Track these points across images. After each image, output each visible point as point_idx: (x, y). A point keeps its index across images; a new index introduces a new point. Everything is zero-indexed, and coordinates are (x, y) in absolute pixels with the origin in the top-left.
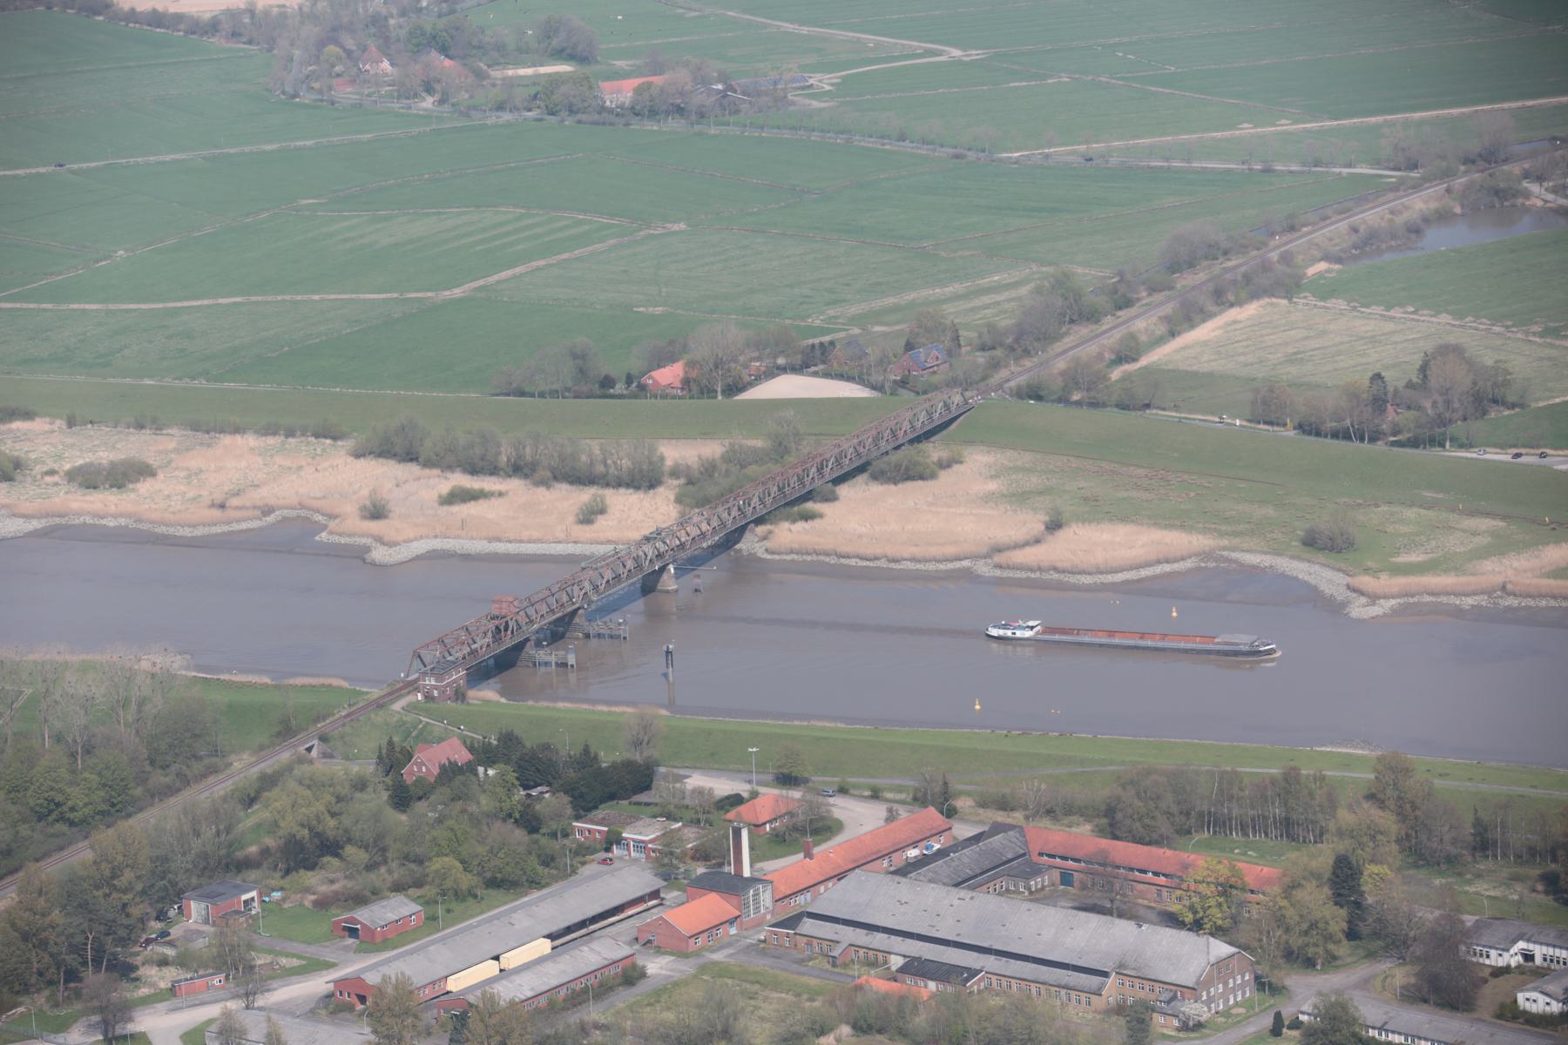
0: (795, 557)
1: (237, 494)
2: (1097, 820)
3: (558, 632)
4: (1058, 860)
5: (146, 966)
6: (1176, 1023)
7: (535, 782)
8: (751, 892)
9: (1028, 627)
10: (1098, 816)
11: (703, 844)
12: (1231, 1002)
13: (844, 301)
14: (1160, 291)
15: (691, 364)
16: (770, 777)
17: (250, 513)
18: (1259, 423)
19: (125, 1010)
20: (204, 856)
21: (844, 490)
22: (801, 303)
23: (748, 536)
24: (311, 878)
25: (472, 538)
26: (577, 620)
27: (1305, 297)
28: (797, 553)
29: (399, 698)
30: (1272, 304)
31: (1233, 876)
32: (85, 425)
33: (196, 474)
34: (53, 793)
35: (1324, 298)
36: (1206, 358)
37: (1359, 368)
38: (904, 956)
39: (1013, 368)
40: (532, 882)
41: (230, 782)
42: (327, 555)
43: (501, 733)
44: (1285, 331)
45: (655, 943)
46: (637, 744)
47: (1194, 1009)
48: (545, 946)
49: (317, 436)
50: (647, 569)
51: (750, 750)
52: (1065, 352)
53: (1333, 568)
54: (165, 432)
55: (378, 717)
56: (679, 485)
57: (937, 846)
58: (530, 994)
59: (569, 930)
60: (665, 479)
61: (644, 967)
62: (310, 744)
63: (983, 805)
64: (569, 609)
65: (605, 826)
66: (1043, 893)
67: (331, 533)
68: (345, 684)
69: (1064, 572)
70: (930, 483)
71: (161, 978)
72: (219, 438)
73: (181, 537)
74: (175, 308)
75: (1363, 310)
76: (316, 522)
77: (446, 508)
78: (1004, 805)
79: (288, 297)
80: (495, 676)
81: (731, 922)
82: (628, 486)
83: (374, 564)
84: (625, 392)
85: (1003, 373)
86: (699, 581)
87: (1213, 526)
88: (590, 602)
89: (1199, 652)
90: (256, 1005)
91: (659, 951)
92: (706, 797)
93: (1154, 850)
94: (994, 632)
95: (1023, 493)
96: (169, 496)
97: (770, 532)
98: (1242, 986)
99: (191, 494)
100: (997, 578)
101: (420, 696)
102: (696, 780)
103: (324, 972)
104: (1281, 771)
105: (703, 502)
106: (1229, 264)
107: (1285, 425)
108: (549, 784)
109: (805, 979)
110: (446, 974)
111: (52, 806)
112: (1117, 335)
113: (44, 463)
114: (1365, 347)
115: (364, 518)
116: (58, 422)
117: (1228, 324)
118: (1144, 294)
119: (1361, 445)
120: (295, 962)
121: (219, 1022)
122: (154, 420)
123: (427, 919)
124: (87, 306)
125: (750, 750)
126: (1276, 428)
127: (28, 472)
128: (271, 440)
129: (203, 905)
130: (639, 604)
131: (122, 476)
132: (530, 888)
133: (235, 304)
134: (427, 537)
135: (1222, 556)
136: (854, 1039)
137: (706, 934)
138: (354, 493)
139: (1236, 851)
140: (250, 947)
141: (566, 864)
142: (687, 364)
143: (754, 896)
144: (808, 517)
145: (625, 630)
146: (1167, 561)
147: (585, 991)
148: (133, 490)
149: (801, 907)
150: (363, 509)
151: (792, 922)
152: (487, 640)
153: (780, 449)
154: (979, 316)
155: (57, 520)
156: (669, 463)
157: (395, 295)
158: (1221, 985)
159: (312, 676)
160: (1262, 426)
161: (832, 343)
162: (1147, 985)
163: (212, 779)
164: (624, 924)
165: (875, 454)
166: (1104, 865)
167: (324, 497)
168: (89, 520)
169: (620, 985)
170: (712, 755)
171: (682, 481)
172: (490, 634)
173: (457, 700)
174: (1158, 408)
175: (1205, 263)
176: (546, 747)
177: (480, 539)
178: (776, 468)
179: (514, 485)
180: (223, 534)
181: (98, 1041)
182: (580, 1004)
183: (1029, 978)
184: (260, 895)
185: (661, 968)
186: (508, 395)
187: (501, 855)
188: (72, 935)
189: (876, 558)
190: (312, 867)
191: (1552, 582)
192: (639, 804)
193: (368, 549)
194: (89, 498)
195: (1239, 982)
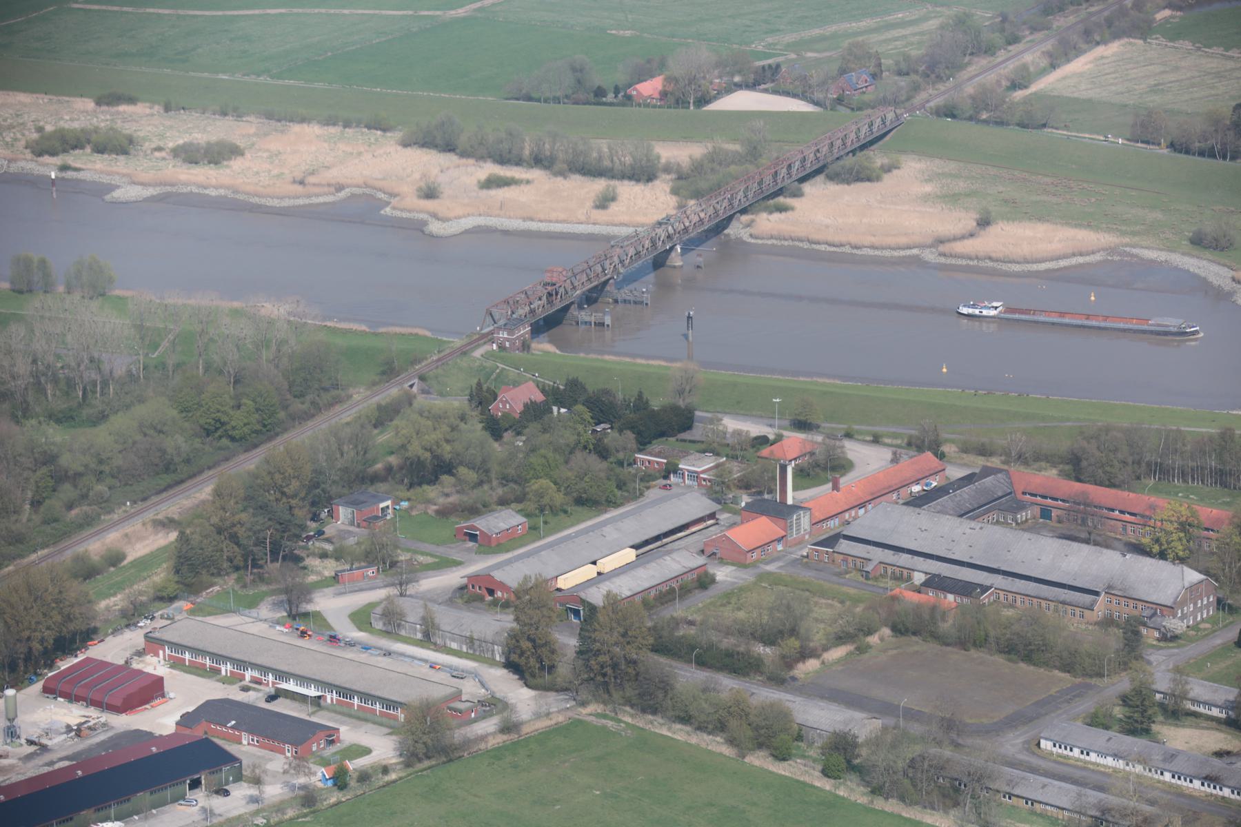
0: (774, 242)
1: (312, 173)
2: (1061, 466)
3: (591, 298)
4: (1039, 498)
5: (310, 558)
6: (1157, 634)
7: (599, 420)
8: (795, 517)
9: (993, 307)
10: (1060, 463)
11: (744, 475)
12: (1199, 619)
13: (778, 30)
14: (1040, 30)
15: (668, 80)
16: (787, 423)
17: (326, 189)
18: (1138, 142)
19: (306, 592)
20: (345, 470)
21: (807, 188)
22: (744, 32)
24: (431, 491)
25: (510, 217)
26: (608, 288)
27: (1156, 39)
28: (776, 239)
29: (479, 346)
30: (1130, 44)
31: (1192, 516)
32: (179, 110)
33: (276, 155)
34: (219, 414)
35: (1171, 40)
36: (1083, 87)
37: (1211, 98)
38: (926, 573)
39: (931, 91)
40: (610, 502)
41: (354, 411)
42: (392, 226)
43: (568, 379)
44: (1144, 66)
45: (718, 556)
46: (681, 393)
47: (1175, 625)
48: (629, 555)
49: (369, 127)
50: (660, 248)
51: (774, 400)
52: (971, 79)
53: (1219, 264)
54: (244, 119)
55: (464, 363)
56: (671, 180)
57: (934, 484)
58: (629, 593)
59: (647, 543)
60: (659, 174)
61: (714, 574)
62: (412, 382)
63: (965, 450)
64: (603, 279)
65: (665, 458)
66: (1027, 524)
67: (394, 208)
68: (428, 334)
69: (997, 260)
70: (875, 184)
71: (328, 568)
72: (290, 126)
73: (271, 207)
74: (233, 16)
75: (1207, 50)
76: (379, 199)
77: (485, 193)
78: (983, 451)
79: (323, 11)
80: (543, 332)
81: (779, 540)
82: (631, 178)
83: (431, 236)
84: (615, 100)
85: (923, 96)
86: (701, 259)
87: (1115, 227)
88: (619, 273)
89: (1136, 331)
90: (408, 593)
91: (722, 562)
92: (743, 438)
93: (1113, 491)
94: (965, 310)
95: (953, 195)
96: (257, 173)
97: (753, 221)
98: (1207, 607)
99: (275, 172)
100: (939, 263)
101: (495, 347)
102: (731, 424)
103: (454, 569)
104: (1219, 431)
105: (697, 195)
106: (1093, 9)
107: (1159, 144)
108: (611, 422)
109: (845, 589)
110: (556, 574)
111: (218, 425)
112: (1011, 66)
113: (150, 140)
114: (1214, 81)
115: (420, 197)
116: (157, 107)
117: (1096, 59)
118: (1027, 33)
119: (1224, 162)
120: (430, 560)
121: (383, 605)
122: (235, 109)
123: (530, 528)
124: (160, 11)
125: (774, 400)
126: (1152, 147)
127: (139, 148)
128: (332, 130)
129: (350, 510)
130: (651, 277)
131: (218, 154)
132: (609, 506)
133: (281, 14)
134: (473, 215)
135: (1125, 251)
136: (894, 640)
137: (760, 550)
138: (408, 176)
139: (1180, 495)
140: (396, 547)
141: (635, 488)
142: (665, 79)
143: (797, 520)
144: (782, 209)
145: (647, 298)
146: (1081, 255)
147: (672, 590)
148: (227, 167)
149: (832, 530)
150: (419, 189)
151: (831, 541)
152: (542, 302)
153: (753, 153)
154: (890, 47)
155: (169, 189)
156: (663, 161)
157: (411, 13)
158: (1192, 605)
159: (401, 326)
160: (1139, 145)
161: (778, 66)
162: (1131, 603)
163: (338, 408)
164: (686, 540)
165: (829, 160)
166: (1085, 504)
167: (384, 179)
168: (195, 190)
169: (696, 588)
170: (738, 402)
171: (673, 176)
172: (544, 298)
173: (524, 350)
174: (1052, 127)
175: (1072, 8)
176: (606, 392)
177: (517, 218)
178: (751, 168)
179: (536, 174)
180: (304, 206)
181: (283, 617)
182: (666, 602)
183: (1032, 594)
184: (394, 503)
185: (726, 576)
186: (517, 99)
187: (586, 479)
188: (259, 531)
190: (433, 481)
192: (684, 441)
193: (425, 223)
194: (192, 171)
195: (1205, 602)
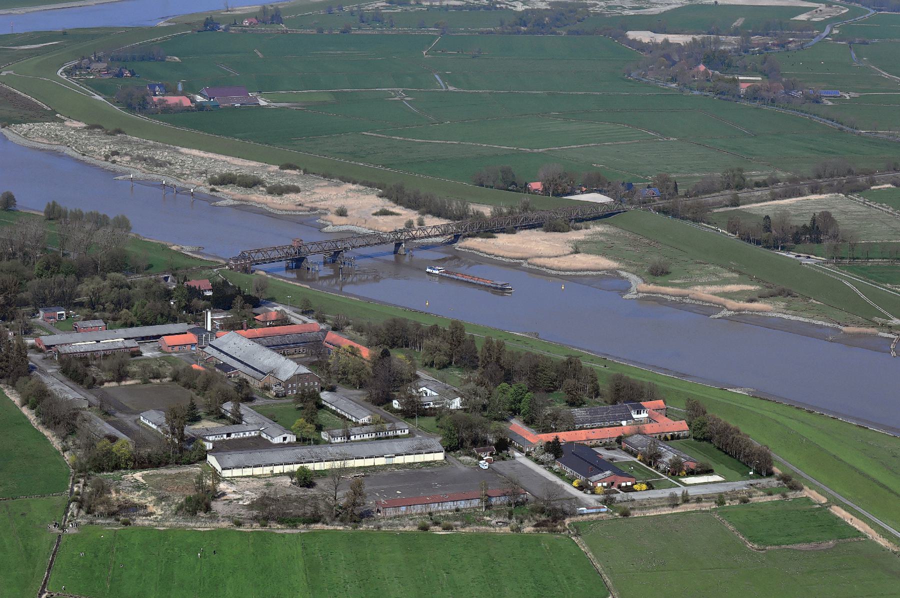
26: (339, 256)
128: (362, 187)
130: (392, 258)
150: (337, 211)
155: (244, 203)
168: (253, 204)
189: (491, 255)
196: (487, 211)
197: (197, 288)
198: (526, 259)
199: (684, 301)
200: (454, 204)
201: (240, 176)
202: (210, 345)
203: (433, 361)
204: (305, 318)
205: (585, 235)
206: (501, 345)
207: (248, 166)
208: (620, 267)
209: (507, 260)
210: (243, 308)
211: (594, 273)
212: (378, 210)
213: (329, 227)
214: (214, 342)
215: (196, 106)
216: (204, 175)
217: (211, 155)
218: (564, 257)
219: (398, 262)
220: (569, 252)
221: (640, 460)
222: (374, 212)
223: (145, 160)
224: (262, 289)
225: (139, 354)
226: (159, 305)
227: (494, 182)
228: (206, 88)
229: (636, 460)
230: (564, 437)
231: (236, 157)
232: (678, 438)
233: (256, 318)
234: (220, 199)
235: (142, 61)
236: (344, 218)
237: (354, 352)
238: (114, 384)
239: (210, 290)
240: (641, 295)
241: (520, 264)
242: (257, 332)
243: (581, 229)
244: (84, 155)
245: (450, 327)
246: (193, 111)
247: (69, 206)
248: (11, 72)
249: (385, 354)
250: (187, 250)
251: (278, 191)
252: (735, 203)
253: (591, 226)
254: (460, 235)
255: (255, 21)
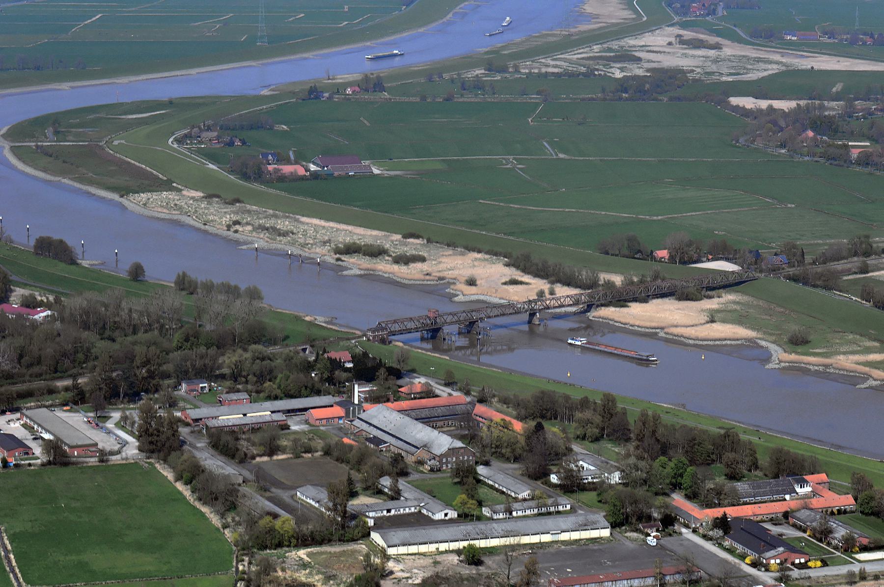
0: (601, 320)
23: (593, 310)
26: (475, 326)
83: (452, 301)
128: (487, 256)
130: (526, 328)
150: (467, 281)
155: (371, 272)
168: (380, 273)
191: (855, 365)
196: (618, 280)
197: (338, 360)
198: (662, 328)
199: (828, 370)
200: (584, 273)
201: (364, 245)
202: (358, 418)
203: (585, 434)
204: (449, 390)
205: (718, 304)
206: (656, 418)
207: (371, 235)
208: (758, 336)
209: (643, 330)
210: (386, 379)
211: (733, 342)
212: (507, 280)
213: (459, 297)
214: (363, 416)
215: (311, 174)
216: (328, 244)
217: (332, 224)
218: (701, 326)
219: (532, 332)
220: (705, 322)
221: (809, 536)
222: (504, 281)
223: (267, 229)
224: (403, 361)
225: (287, 427)
226: (301, 375)
227: (619, 250)
228: (319, 157)
229: (805, 535)
230: (732, 512)
231: (356, 226)
232: (845, 512)
233: (400, 390)
234: (347, 269)
235: (250, 130)
236: (474, 288)
237: (506, 426)
238: (265, 459)
239: (349, 362)
240: (783, 364)
241: (656, 334)
242: (404, 404)
243: (713, 297)
244: (205, 224)
245: (601, 400)
246: (307, 179)
247: (199, 276)
248: (123, 141)
249: (539, 427)
250: (320, 320)
251: (404, 260)
252: (864, 270)
253: (723, 295)
254: (594, 304)
255: (357, 89)
